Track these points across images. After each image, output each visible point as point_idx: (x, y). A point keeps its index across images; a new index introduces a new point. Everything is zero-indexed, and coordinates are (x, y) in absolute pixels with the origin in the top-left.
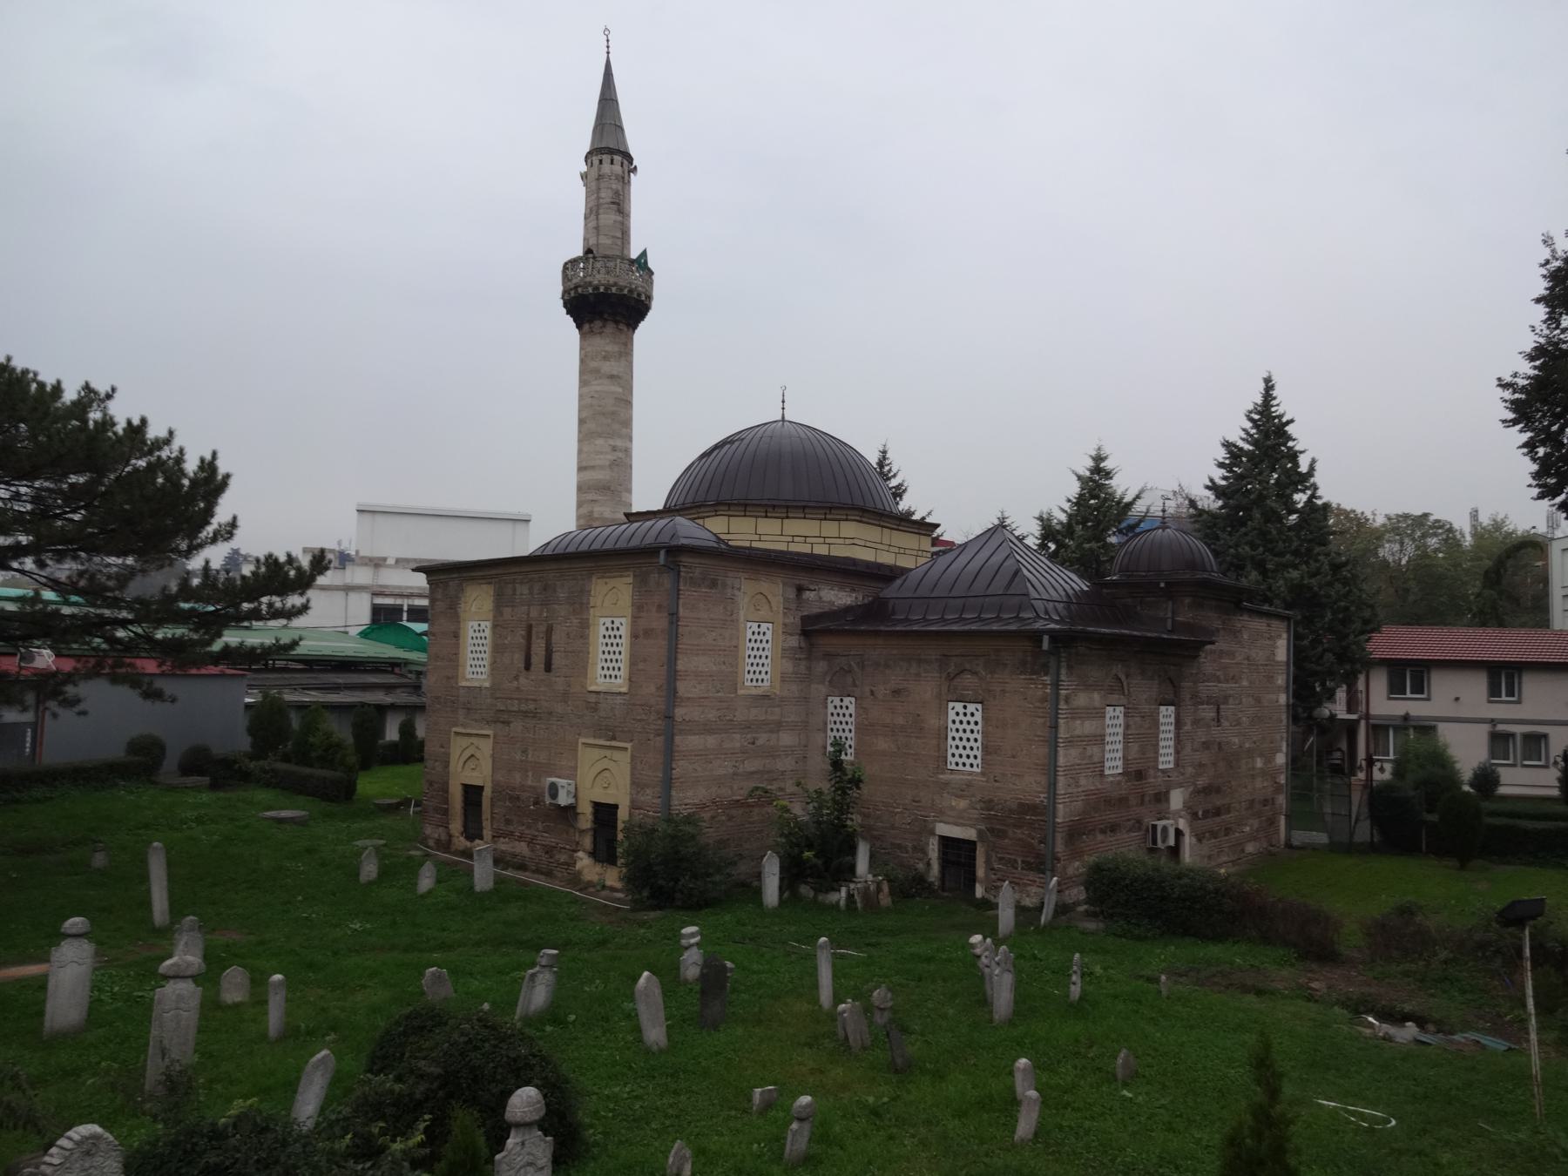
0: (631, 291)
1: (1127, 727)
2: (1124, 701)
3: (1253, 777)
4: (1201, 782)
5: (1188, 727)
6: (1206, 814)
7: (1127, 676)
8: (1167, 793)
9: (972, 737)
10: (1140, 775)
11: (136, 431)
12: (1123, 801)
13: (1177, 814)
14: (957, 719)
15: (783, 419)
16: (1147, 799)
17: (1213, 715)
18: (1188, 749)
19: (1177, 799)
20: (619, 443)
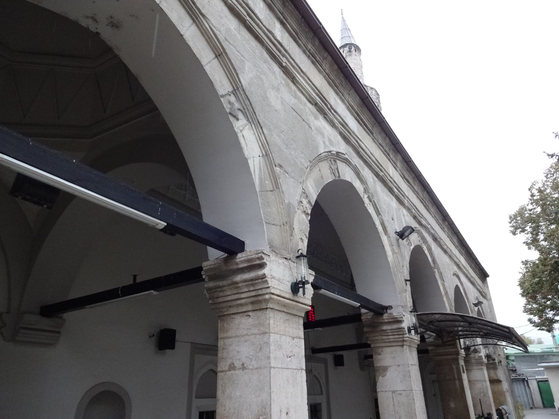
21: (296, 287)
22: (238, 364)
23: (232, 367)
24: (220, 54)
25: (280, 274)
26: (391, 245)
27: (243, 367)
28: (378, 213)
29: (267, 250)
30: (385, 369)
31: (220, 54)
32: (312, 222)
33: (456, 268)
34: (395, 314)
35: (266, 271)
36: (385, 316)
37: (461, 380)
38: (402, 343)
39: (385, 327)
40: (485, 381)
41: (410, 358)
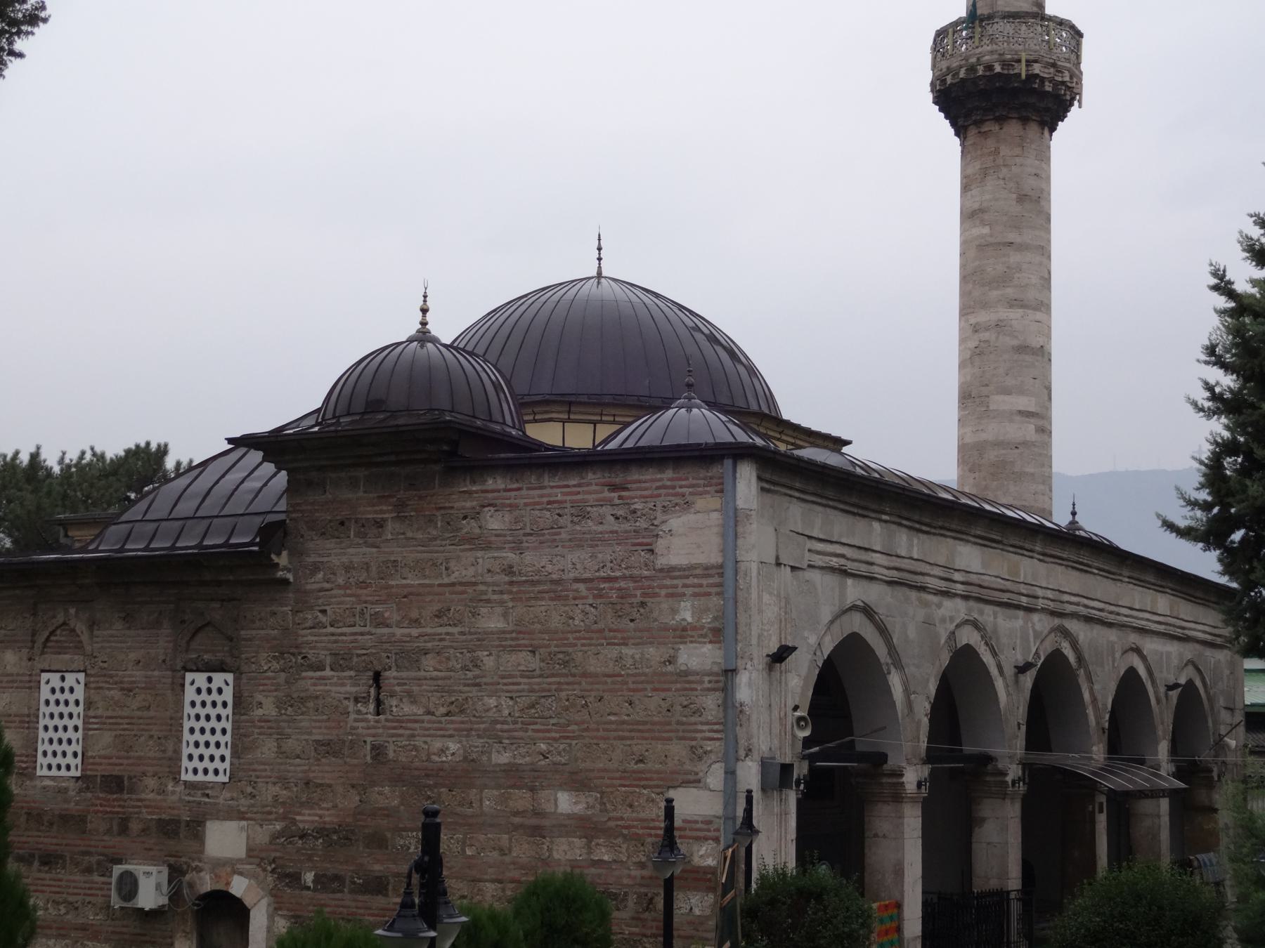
0: (972, 69)
1: (89, 704)
2: (78, 660)
3: (537, 832)
4: (307, 819)
5: (267, 708)
6: (325, 882)
7: (92, 624)
8: (201, 823)
9: (70, 724)
10: (115, 784)
11: (1222, 404)
12: (72, 822)
13: (233, 867)
14: (52, 699)
15: (599, 275)
16: (135, 826)
17: (363, 685)
18: (267, 749)
19: (225, 840)
20: (983, 317)
21: (919, 785)
22: (881, 834)
23: (876, 835)
24: (883, 631)
25: (912, 777)
26: (1007, 686)
27: (884, 836)
28: (994, 654)
29: (904, 765)
30: (983, 820)
31: (883, 631)
32: (930, 720)
33: (1133, 638)
34: (1000, 766)
35: (904, 779)
36: (990, 767)
37: (1093, 822)
38: (1004, 796)
39: (988, 779)
40: (1159, 816)
41: (1012, 813)
